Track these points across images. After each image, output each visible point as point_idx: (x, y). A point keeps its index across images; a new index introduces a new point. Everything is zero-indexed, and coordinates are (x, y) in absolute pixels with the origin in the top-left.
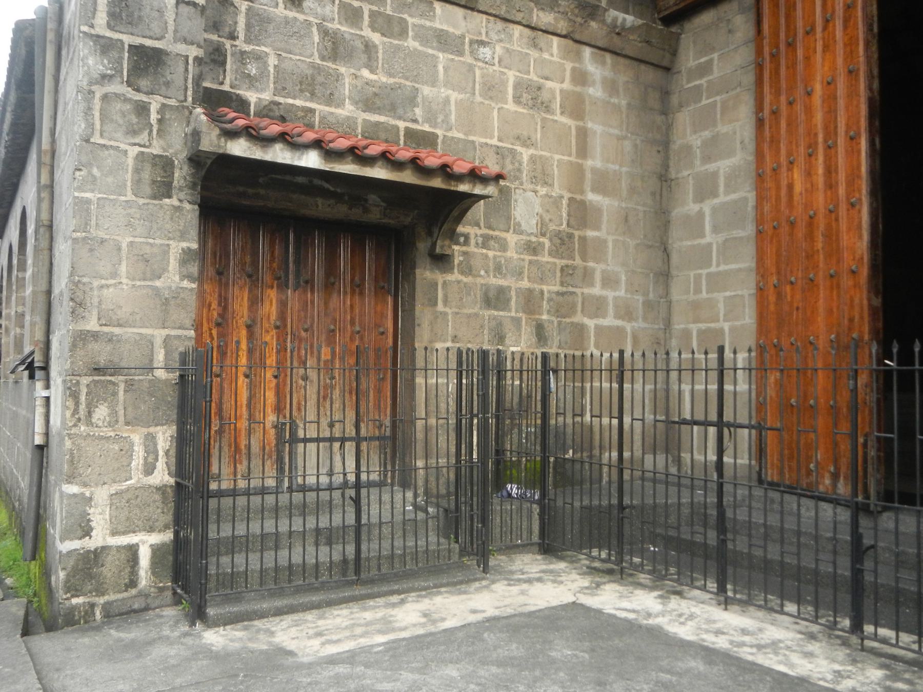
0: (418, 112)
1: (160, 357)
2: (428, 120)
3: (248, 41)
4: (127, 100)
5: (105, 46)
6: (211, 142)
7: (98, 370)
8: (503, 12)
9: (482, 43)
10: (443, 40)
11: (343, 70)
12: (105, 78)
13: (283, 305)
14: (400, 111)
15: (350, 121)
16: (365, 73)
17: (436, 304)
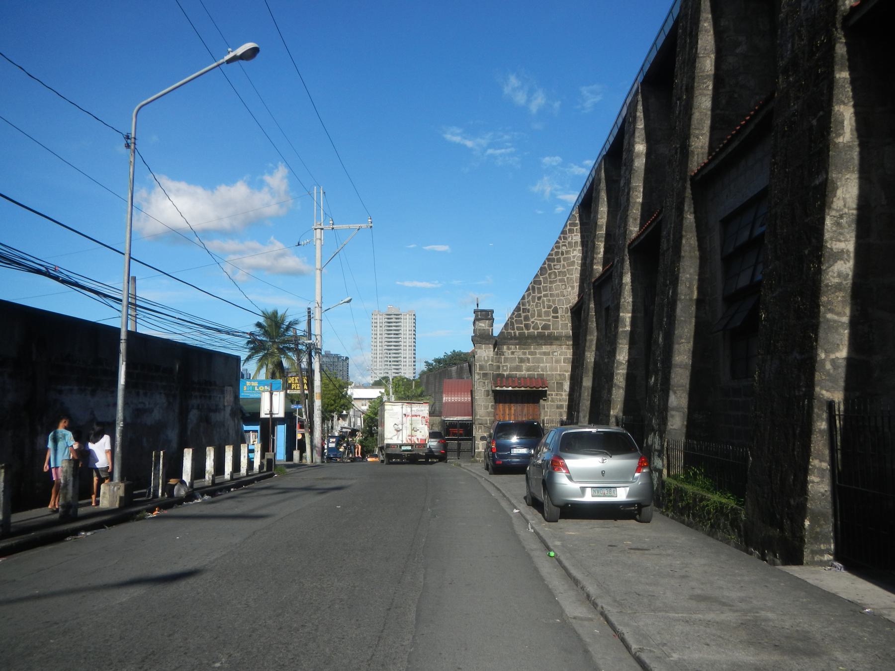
0: (540, 370)
1: (488, 422)
2: (541, 371)
3: (504, 363)
4: (482, 382)
5: (479, 374)
6: (494, 388)
7: (480, 424)
8: (559, 344)
9: (555, 352)
10: (545, 354)
11: (523, 364)
12: (479, 379)
13: (514, 410)
14: (535, 370)
15: (525, 374)
16: (528, 364)
17: (545, 409)
